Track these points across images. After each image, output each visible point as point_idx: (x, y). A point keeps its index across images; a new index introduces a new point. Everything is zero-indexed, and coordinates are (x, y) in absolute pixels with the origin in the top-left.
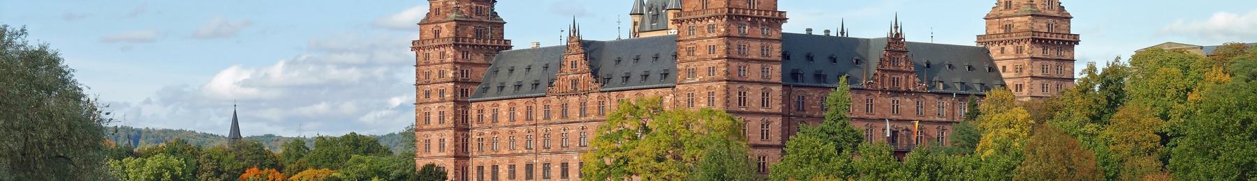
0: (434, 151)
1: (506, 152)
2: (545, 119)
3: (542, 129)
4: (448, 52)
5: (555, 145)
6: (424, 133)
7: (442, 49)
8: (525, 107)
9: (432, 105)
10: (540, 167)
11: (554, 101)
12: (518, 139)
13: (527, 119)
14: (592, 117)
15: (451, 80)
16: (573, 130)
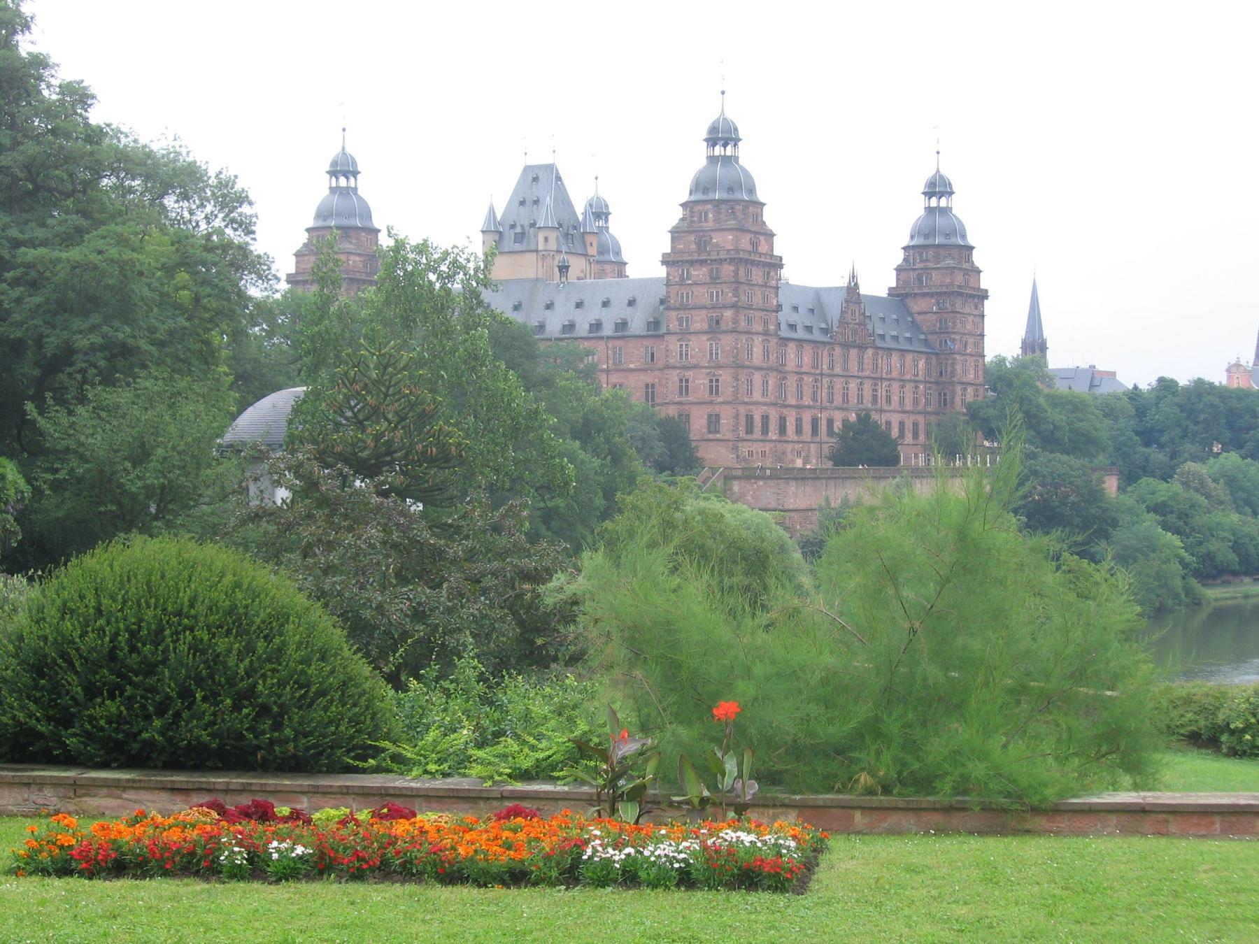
0: (757, 396)
1: (793, 402)
2: (829, 369)
3: (826, 381)
4: (772, 274)
5: (838, 400)
6: (745, 371)
7: (767, 269)
8: (811, 352)
9: (755, 337)
10: (824, 422)
11: (838, 350)
12: (805, 388)
13: (813, 367)
14: (867, 373)
15: (775, 308)
16: (853, 385)
